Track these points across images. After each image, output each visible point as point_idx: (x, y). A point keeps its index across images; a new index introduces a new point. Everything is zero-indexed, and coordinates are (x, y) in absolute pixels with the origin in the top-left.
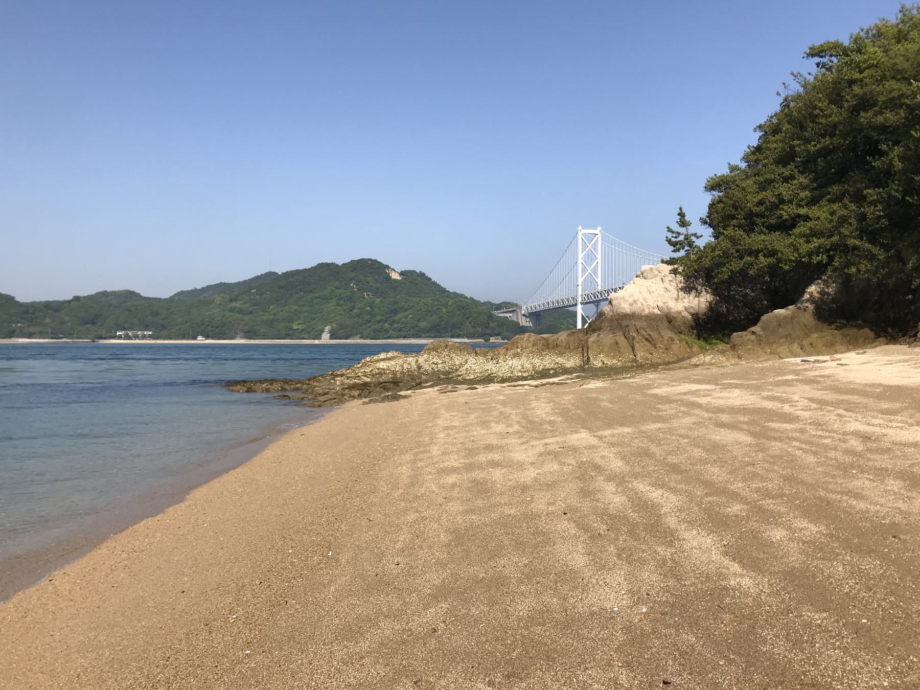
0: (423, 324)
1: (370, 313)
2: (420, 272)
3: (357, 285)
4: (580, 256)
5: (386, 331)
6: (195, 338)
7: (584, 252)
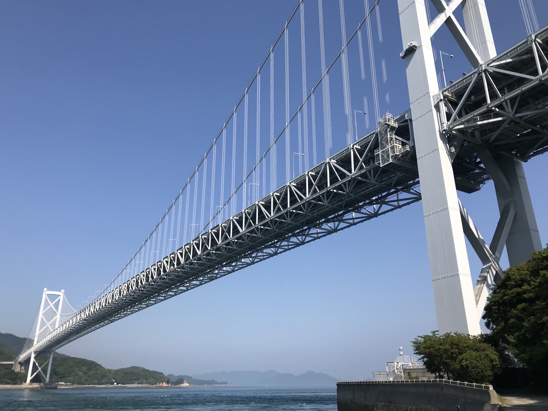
7: (45, 310)
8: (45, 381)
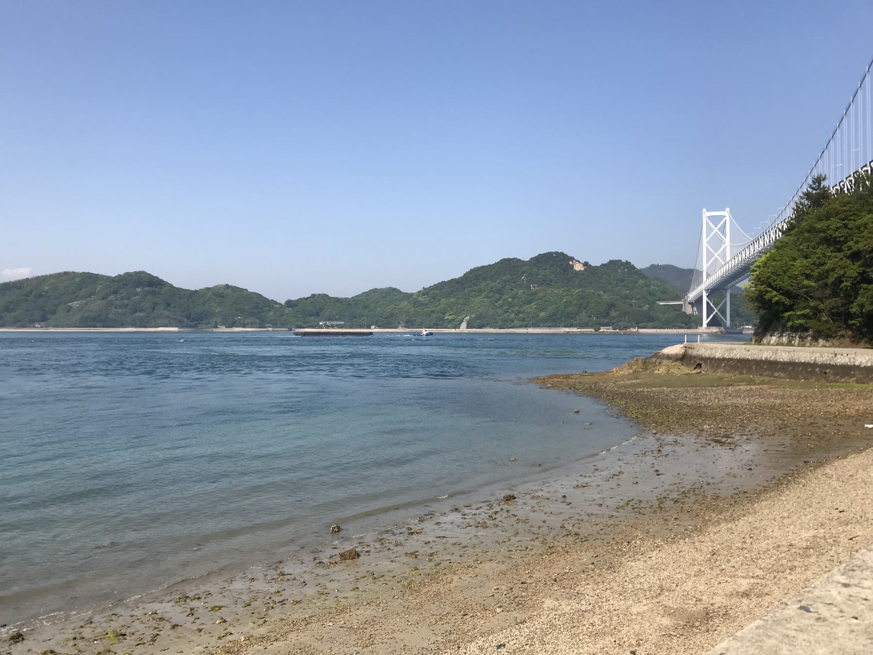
0: (542, 314)
1: (510, 303)
2: (626, 261)
3: (526, 277)
4: (705, 240)
5: (512, 321)
6: (369, 327)
8: (726, 324)
